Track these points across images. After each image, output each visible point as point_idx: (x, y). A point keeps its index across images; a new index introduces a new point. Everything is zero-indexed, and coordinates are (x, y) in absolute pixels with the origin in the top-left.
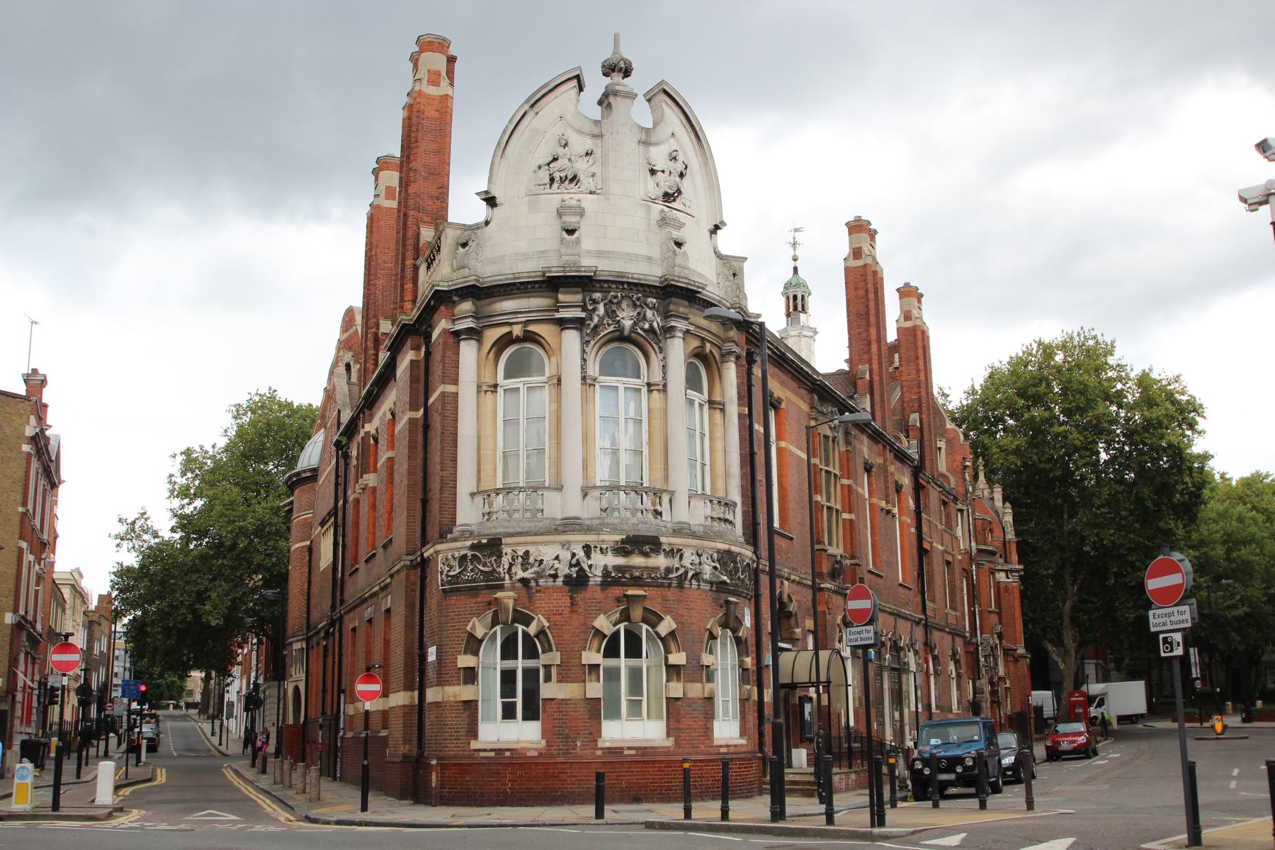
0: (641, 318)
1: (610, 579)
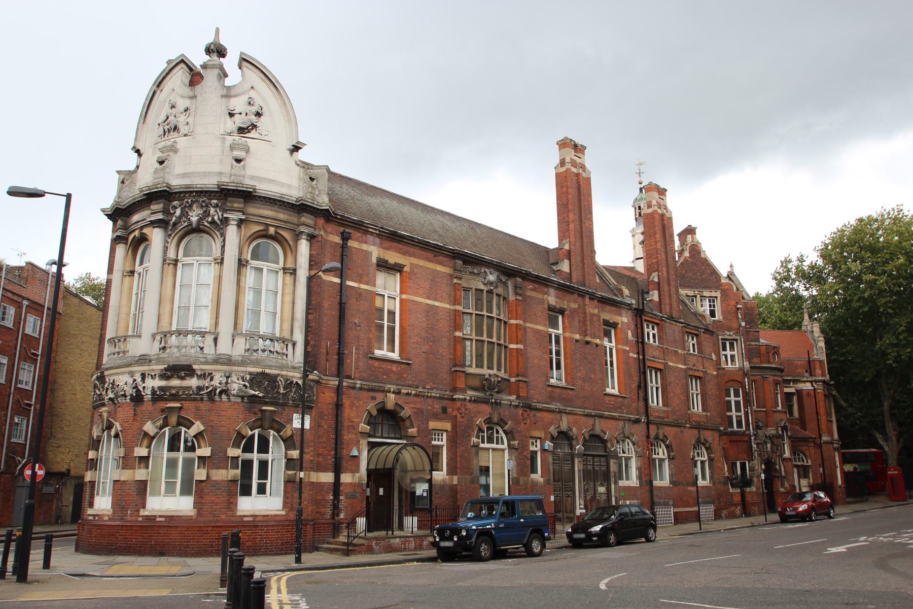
0: (206, 214)
1: (159, 396)
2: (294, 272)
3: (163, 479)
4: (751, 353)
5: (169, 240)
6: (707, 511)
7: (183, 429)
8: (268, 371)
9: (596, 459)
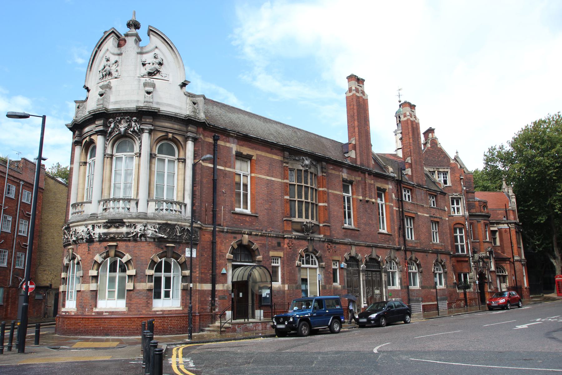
0: (130, 126)
1: (103, 239)
2: (184, 161)
4: (469, 206)
5: (108, 143)
6: (443, 306)
7: (119, 259)
8: (169, 222)
9: (374, 273)
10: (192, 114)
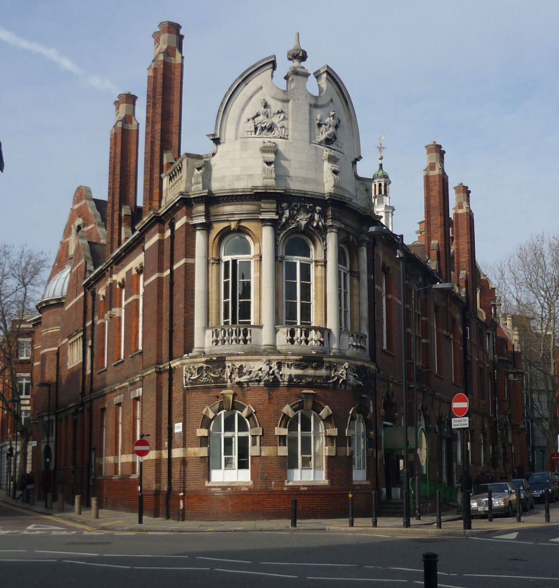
0: (312, 219)
1: (293, 383)
3: (223, 455)
10: (271, 182)
